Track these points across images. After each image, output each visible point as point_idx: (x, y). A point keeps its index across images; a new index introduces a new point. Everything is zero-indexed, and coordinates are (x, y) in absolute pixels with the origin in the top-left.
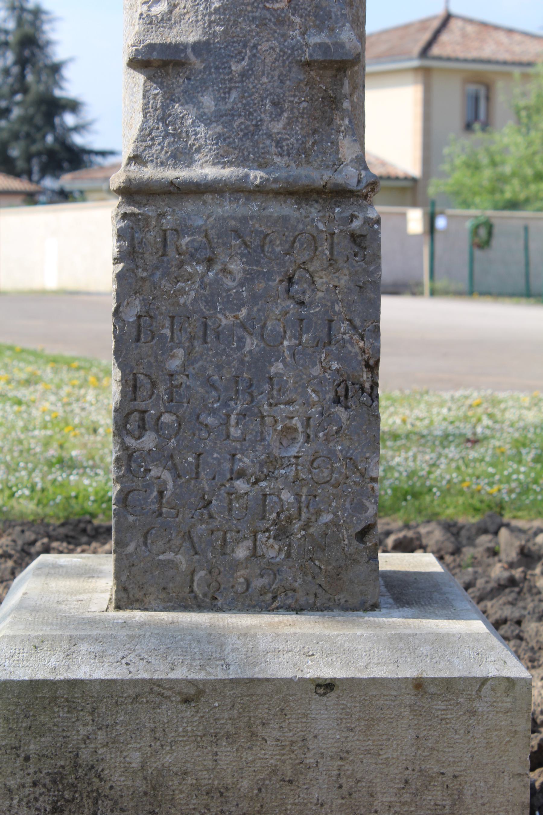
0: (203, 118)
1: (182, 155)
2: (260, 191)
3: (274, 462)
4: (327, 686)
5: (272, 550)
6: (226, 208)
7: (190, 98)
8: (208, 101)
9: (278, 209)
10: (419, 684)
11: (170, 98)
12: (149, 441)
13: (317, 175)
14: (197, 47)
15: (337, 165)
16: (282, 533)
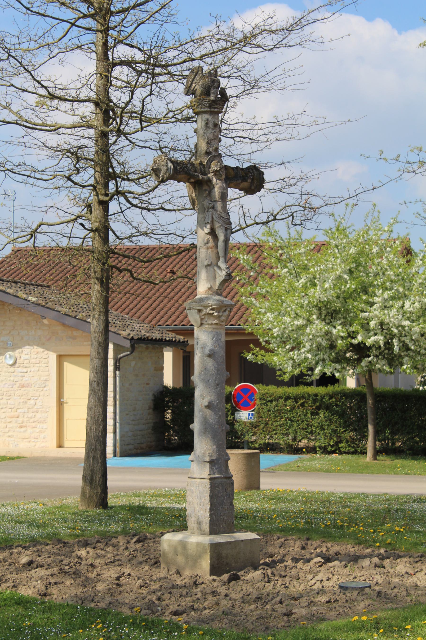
0: (216, 469)
1: (214, 474)
2: (223, 478)
3: (224, 514)
4: (242, 541)
5: (224, 525)
6: (219, 480)
7: (214, 466)
8: (217, 466)
9: (225, 480)
10: (250, 540)
11: (212, 466)
12: (213, 512)
13: (228, 476)
14: (216, 459)
15: (229, 474)
16: (225, 523)
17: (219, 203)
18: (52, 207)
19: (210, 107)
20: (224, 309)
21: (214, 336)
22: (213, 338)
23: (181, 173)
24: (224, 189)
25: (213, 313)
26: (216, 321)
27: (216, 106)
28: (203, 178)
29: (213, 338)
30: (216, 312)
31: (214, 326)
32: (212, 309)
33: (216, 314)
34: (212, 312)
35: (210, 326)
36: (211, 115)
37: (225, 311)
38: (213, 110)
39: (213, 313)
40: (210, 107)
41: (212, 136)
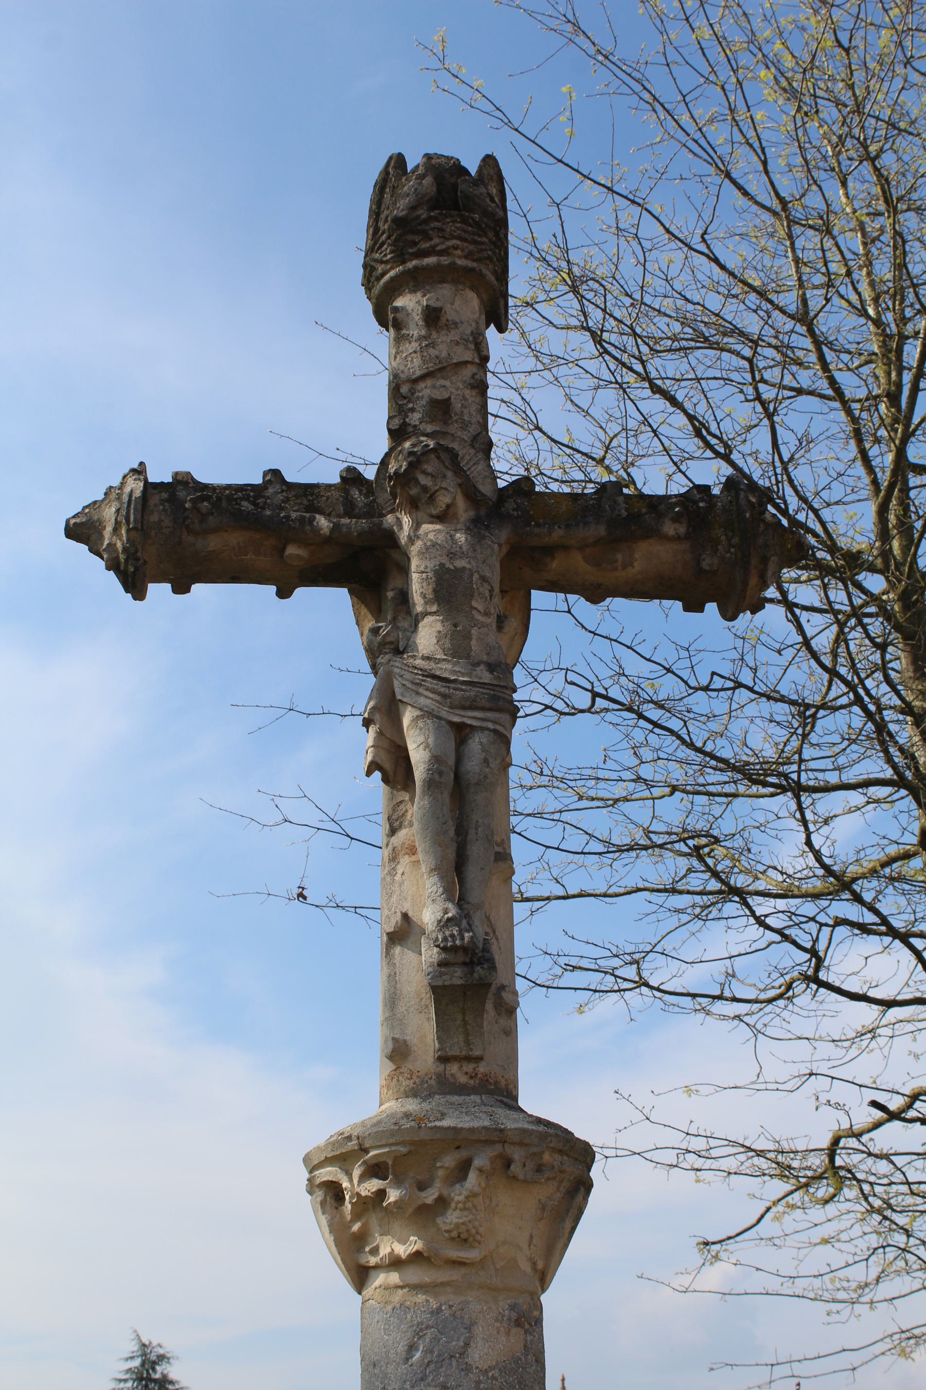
17: (429, 619)
18: (811, 1074)
19: (400, 257)
20: (449, 1161)
21: (419, 1333)
22: (412, 1348)
23: (212, 521)
24: (452, 555)
25: (381, 1194)
26: (414, 1244)
27: (425, 245)
28: (336, 527)
29: (412, 1348)
30: (398, 1182)
31: (415, 1275)
32: (375, 1170)
33: (393, 1195)
34: (374, 1185)
35: (394, 1277)
36: (413, 291)
37: (463, 1168)
38: (411, 265)
39: (381, 1194)
40: (400, 257)
41: (417, 361)
